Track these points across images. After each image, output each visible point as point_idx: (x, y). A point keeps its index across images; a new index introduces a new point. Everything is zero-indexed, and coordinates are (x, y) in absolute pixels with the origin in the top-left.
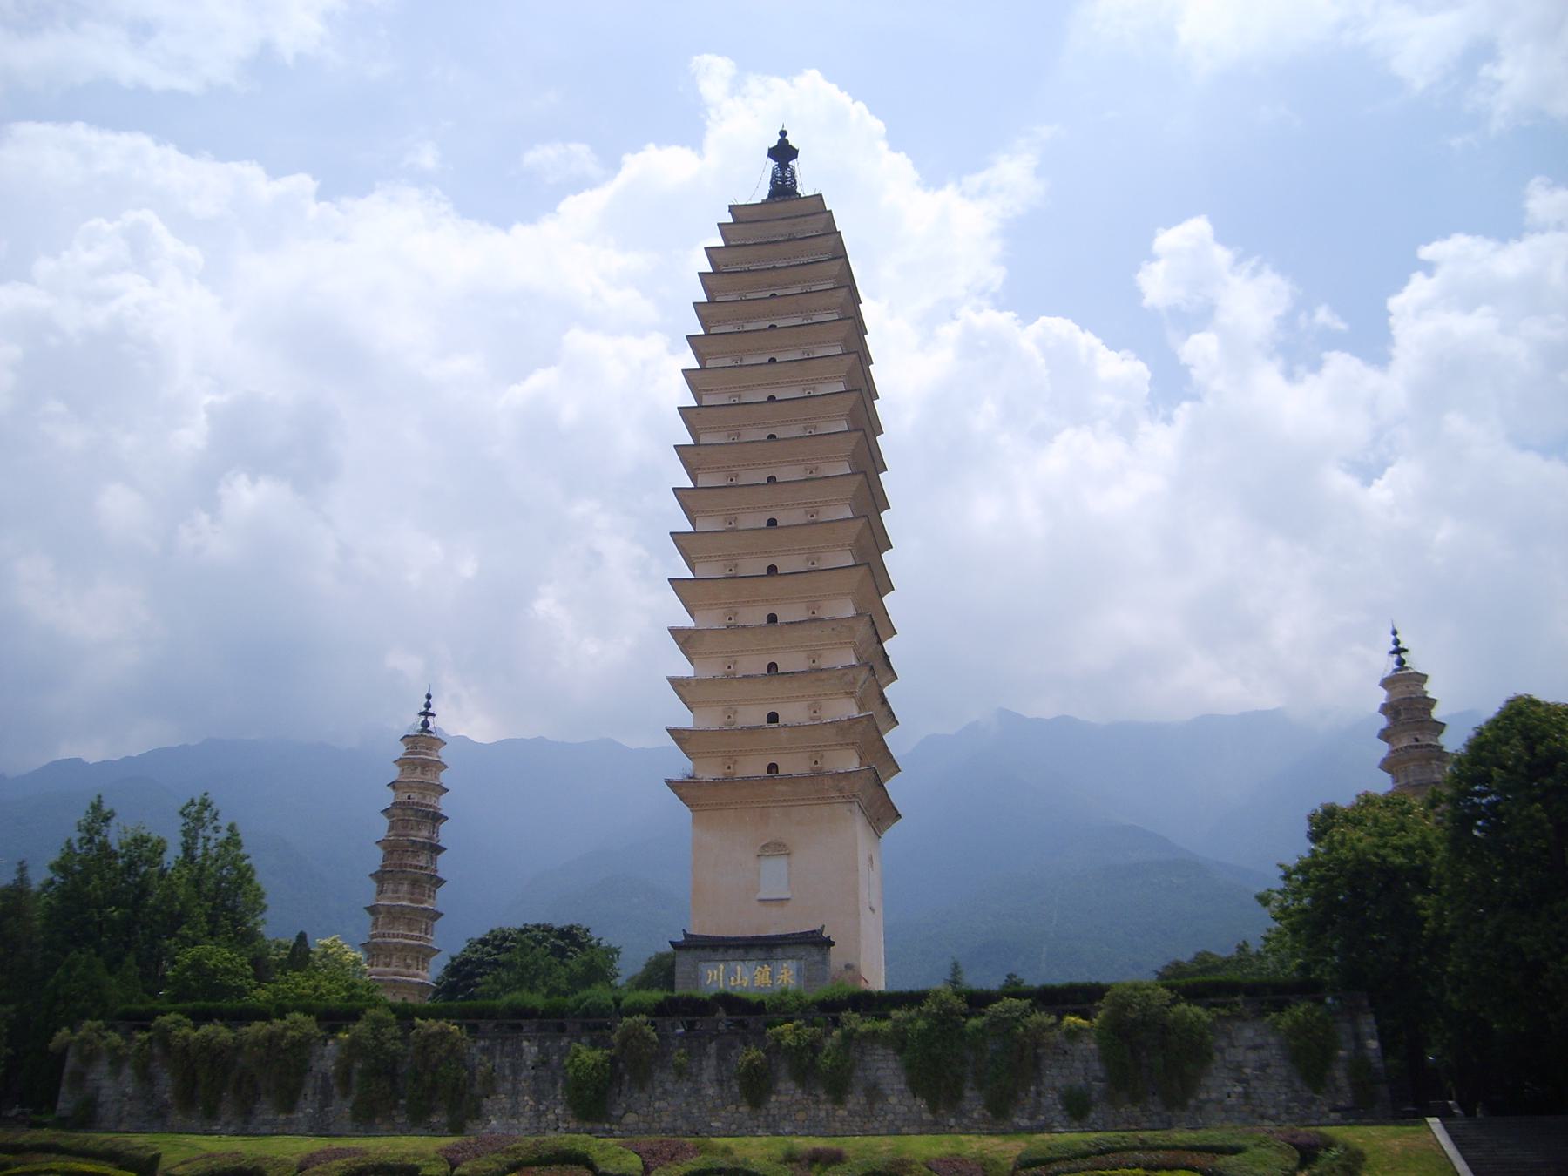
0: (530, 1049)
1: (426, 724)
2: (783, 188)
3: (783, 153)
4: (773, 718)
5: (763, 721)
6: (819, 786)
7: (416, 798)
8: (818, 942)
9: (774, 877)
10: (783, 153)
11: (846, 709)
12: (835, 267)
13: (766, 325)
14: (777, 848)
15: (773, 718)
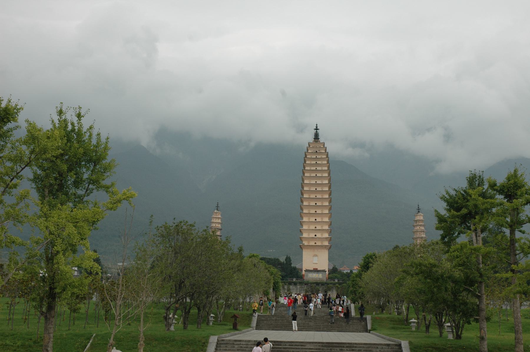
0: (298, 287)
1: (217, 209)
2: (316, 137)
3: (317, 129)
4: (316, 235)
5: (314, 236)
6: (322, 247)
7: (217, 225)
8: (324, 271)
9: (315, 260)
10: (317, 129)
11: (326, 235)
12: (327, 159)
13: (314, 168)
14: (316, 256)
15: (316, 235)
